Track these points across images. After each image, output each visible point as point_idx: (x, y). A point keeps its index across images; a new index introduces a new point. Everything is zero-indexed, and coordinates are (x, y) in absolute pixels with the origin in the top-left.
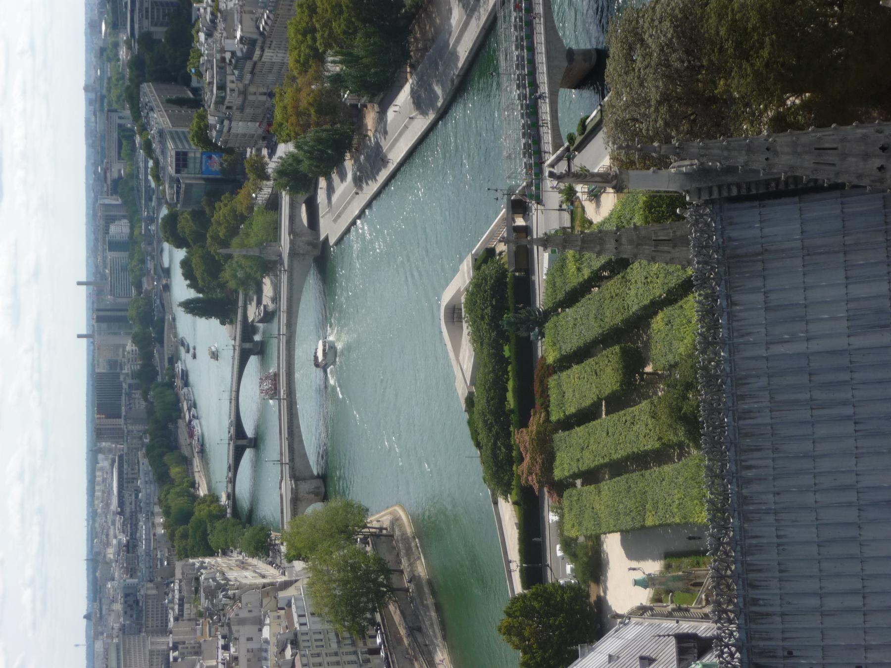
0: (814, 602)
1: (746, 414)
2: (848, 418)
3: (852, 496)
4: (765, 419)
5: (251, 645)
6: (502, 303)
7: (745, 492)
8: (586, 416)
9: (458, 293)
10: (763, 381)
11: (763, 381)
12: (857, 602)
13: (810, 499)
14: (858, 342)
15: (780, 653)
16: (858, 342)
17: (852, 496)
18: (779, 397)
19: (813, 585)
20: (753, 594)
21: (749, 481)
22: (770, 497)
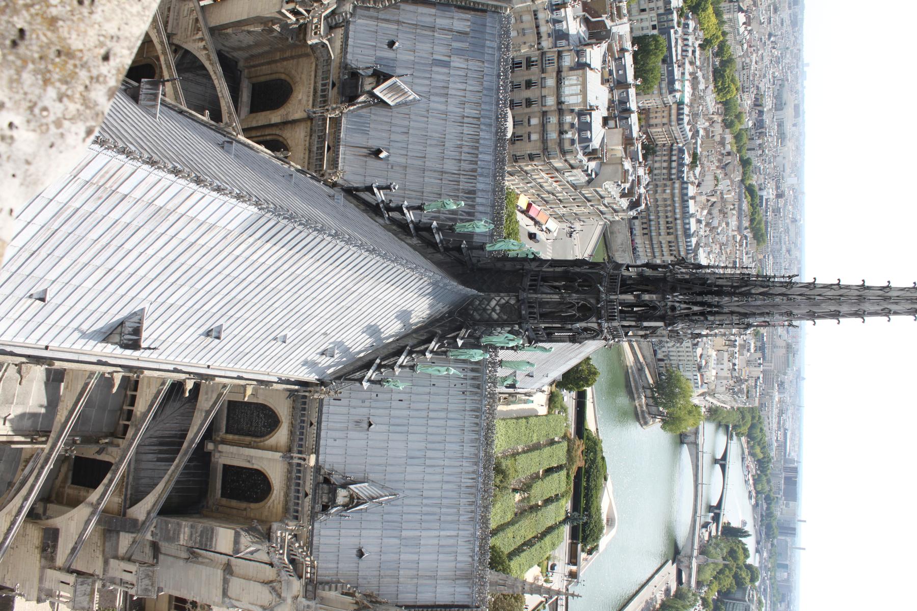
0: (451, 415)
1: (472, 504)
2: (426, 498)
3: (428, 462)
4: (463, 501)
5: (721, 367)
6: (584, 530)
7: (475, 467)
8: (549, 471)
9: (607, 533)
10: (462, 518)
11: (462, 518)
12: (431, 414)
13: (447, 462)
14: (417, 533)
15: (468, 393)
16: (417, 533)
17: (428, 462)
18: (455, 510)
19: (450, 423)
20: (477, 421)
21: (473, 472)
22: (464, 464)
